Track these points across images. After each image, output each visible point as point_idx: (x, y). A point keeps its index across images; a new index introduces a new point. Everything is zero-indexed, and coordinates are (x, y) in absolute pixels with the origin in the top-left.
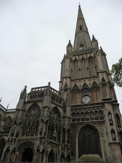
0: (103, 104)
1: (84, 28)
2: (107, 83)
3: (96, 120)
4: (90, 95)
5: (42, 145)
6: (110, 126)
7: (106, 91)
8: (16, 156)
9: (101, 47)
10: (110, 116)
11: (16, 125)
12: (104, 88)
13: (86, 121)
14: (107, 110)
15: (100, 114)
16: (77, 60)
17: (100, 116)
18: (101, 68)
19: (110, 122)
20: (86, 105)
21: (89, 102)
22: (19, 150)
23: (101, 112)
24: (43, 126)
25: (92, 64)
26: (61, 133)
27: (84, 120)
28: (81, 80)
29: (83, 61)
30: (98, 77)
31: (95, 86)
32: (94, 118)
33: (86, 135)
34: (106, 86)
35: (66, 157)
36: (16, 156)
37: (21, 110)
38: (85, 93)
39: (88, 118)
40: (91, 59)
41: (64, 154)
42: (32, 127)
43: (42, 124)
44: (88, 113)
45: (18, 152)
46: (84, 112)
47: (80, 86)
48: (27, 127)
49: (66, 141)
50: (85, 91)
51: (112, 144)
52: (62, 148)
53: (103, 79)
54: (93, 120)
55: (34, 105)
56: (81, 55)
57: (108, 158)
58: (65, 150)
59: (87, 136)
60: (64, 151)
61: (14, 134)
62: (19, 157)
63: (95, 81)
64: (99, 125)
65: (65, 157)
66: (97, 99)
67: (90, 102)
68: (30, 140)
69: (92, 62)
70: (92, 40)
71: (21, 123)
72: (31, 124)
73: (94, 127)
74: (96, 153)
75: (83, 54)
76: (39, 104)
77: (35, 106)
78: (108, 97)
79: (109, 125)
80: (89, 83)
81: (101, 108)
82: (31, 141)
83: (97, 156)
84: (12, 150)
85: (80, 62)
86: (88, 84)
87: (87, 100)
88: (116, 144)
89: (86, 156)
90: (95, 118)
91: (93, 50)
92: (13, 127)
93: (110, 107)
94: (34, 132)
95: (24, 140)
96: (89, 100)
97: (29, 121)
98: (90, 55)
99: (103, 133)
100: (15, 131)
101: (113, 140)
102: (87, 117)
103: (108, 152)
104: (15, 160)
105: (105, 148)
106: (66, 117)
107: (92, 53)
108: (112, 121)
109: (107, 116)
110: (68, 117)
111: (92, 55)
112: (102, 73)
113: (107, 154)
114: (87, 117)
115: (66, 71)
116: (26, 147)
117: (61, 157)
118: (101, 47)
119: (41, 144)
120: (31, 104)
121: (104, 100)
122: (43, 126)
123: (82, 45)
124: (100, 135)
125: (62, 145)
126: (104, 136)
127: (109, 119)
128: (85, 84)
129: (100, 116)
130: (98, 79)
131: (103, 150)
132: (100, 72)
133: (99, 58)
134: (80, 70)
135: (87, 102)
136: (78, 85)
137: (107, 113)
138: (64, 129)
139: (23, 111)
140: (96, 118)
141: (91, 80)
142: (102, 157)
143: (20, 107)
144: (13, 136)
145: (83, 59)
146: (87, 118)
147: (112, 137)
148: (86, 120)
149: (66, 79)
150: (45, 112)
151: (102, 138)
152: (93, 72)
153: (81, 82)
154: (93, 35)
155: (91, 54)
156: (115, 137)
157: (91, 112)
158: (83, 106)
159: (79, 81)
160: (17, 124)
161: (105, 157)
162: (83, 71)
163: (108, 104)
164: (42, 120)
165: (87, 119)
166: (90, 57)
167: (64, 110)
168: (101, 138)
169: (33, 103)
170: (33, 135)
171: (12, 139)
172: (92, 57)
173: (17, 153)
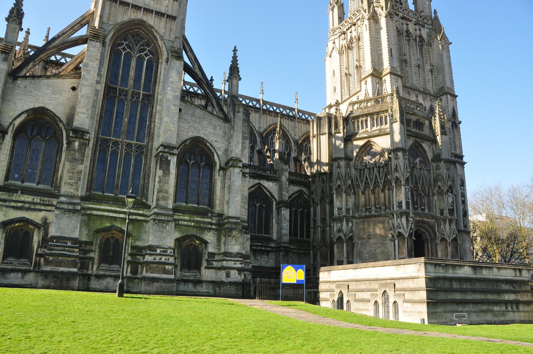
76: (425, 145)
82: (428, 220)
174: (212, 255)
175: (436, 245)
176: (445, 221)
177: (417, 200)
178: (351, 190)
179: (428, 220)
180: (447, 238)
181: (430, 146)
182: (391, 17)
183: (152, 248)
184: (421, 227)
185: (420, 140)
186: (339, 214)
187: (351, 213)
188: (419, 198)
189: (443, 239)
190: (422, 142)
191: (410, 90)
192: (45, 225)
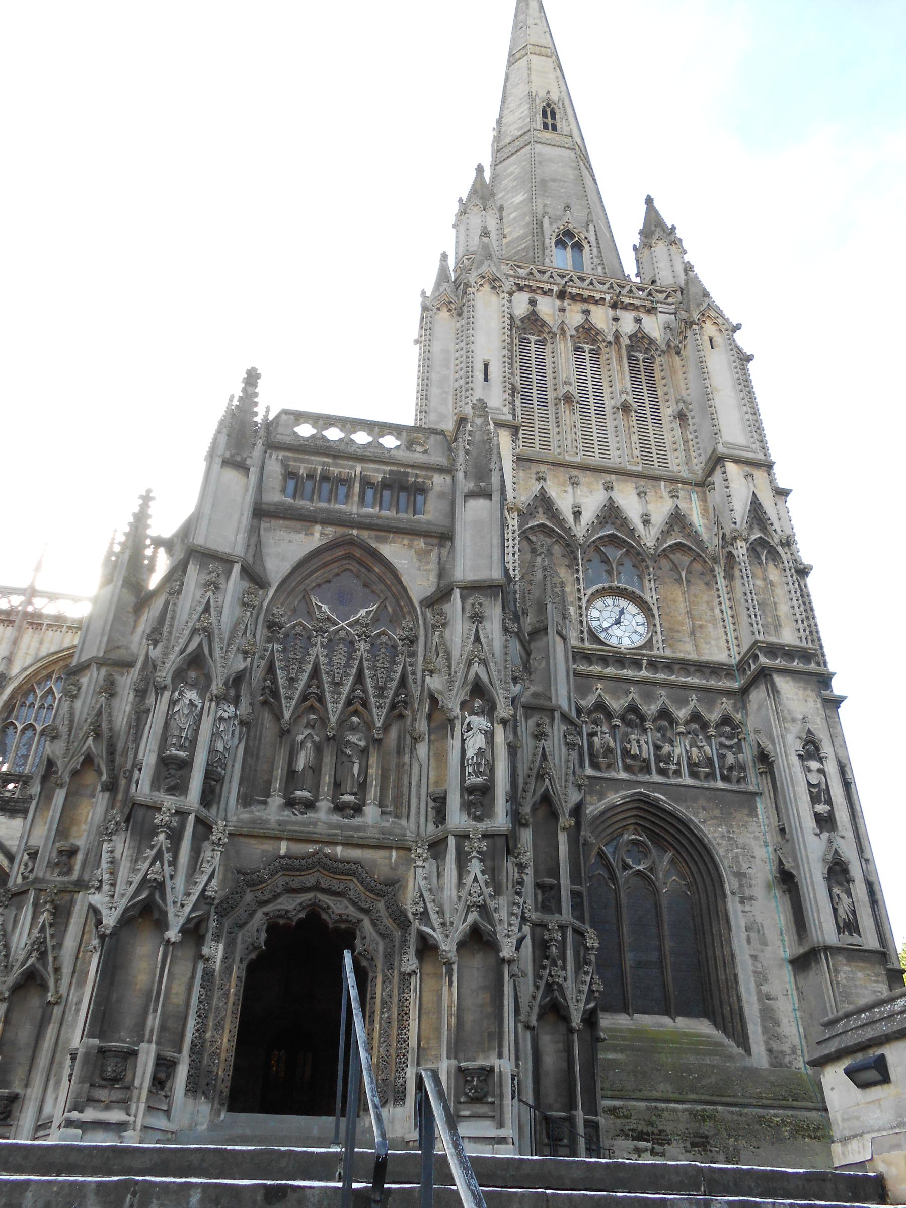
0: (764, 675)
2: (782, 544)
3: (694, 775)
4: (650, 597)
5: (503, 901)
6: (816, 834)
7: (772, 591)
8: (208, 975)
10: (814, 765)
11: (203, 687)
12: (758, 571)
13: (623, 775)
14: (794, 720)
15: (723, 740)
16: (544, 324)
17: (722, 757)
19: (822, 808)
20: (620, 659)
21: (639, 641)
22: (227, 922)
23: (728, 729)
24: (490, 736)
25: (652, 388)
26: (526, 825)
27: (609, 766)
28: (585, 478)
29: (587, 347)
30: (703, 484)
31: (679, 546)
32: (678, 764)
33: (622, 876)
34: (771, 565)
35: (576, 1020)
36: (208, 975)
37: (237, 568)
38: (609, 573)
39: (645, 755)
40: (641, 356)
41: (566, 1000)
42: (337, 741)
43: (479, 722)
44: (642, 718)
45: (221, 947)
46: (616, 704)
47: (577, 514)
48: (284, 733)
49: (565, 894)
50: (606, 561)
51: (841, 959)
52: (542, 947)
54: (677, 773)
55: (340, 552)
56: (575, 298)
57: (786, 1048)
58: (564, 968)
59: (627, 882)
60: (563, 973)
61: (186, 765)
62: (226, 995)
63: (682, 505)
64: (717, 813)
65: (565, 1019)
66: (693, 633)
67: (649, 644)
68: (347, 844)
69: (650, 372)
71: (238, 680)
72: (334, 710)
73: (685, 824)
74: (688, 1014)
76: (396, 552)
77: (350, 560)
78: (788, 637)
79: (809, 823)
80: (646, 511)
81: (726, 705)
82: (356, 853)
83: (703, 1027)
84: (189, 920)
87: (623, 628)
88: (863, 960)
90: (691, 765)
91: (661, 297)
92: (173, 703)
93: (811, 704)
94: (363, 786)
95: (281, 839)
96: (641, 629)
97: (304, 677)
98: (638, 320)
99: (744, 875)
100: (193, 742)
101: (839, 933)
102: (643, 745)
103: (786, 1009)
104: (202, 1016)
105: (761, 978)
106: (550, 711)
107: (650, 311)
108: (829, 802)
109: (795, 760)
110: (565, 718)
111: (654, 326)
112: (748, 469)
113: (777, 1023)
114: (643, 745)
115: (480, 376)
116: (290, 905)
117: (540, 1017)
119: (498, 892)
120: (316, 537)
121: (773, 650)
122: (490, 736)
123: (569, 233)
124: (730, 884)
126: (751, 898)
127: (810, 784)
128: (611, 513)
129: (722, 757)
130: (704, 500)
131: (748, 989)
132: (737, 461)
133: (718, 364)
134: (568, 398)
135: (626, 642)
137: (794, 745)
138: (546, 799)
139: (254, 577)
140: (697, 765)
141: (651, 495)
142: (743, 1041)
143: (230, 538)
144: (179, 788)
145: (588, 332)
146: (635, 750)
147: (835, 910)
148: (628, 768)
150: (487, 624)
151: (739, 907)
152: (661, 447)
153: (581, 491)
156: (854, 912)
157: (664, 714)
158: (604, 660)
159: (563, 474)
160: (217, 687)
161: (767, 1043)
162: (585, 415)
163: (793, 678)
164: (478, 689)
165: (634, 757)
167: (524, 655)
168: (733, 906)
169: (330, 530)
170: (358, 809)
171: (181, 814)
172: (652, 341)
173: (215, 951)
175: (406, 977)
176: (437, 847)
177: (315, 769)
178: (100, 773)
179: (356, 853)
180: (437, 935)
181: (422, 555)
182: (494, 288)
184: (317, 888)
185: (365, 535)
186: (24, 878)
187: (77, 867)
188: (328, 760)
189: (427, 948)
190: (384, 540)
191: (575, 472)
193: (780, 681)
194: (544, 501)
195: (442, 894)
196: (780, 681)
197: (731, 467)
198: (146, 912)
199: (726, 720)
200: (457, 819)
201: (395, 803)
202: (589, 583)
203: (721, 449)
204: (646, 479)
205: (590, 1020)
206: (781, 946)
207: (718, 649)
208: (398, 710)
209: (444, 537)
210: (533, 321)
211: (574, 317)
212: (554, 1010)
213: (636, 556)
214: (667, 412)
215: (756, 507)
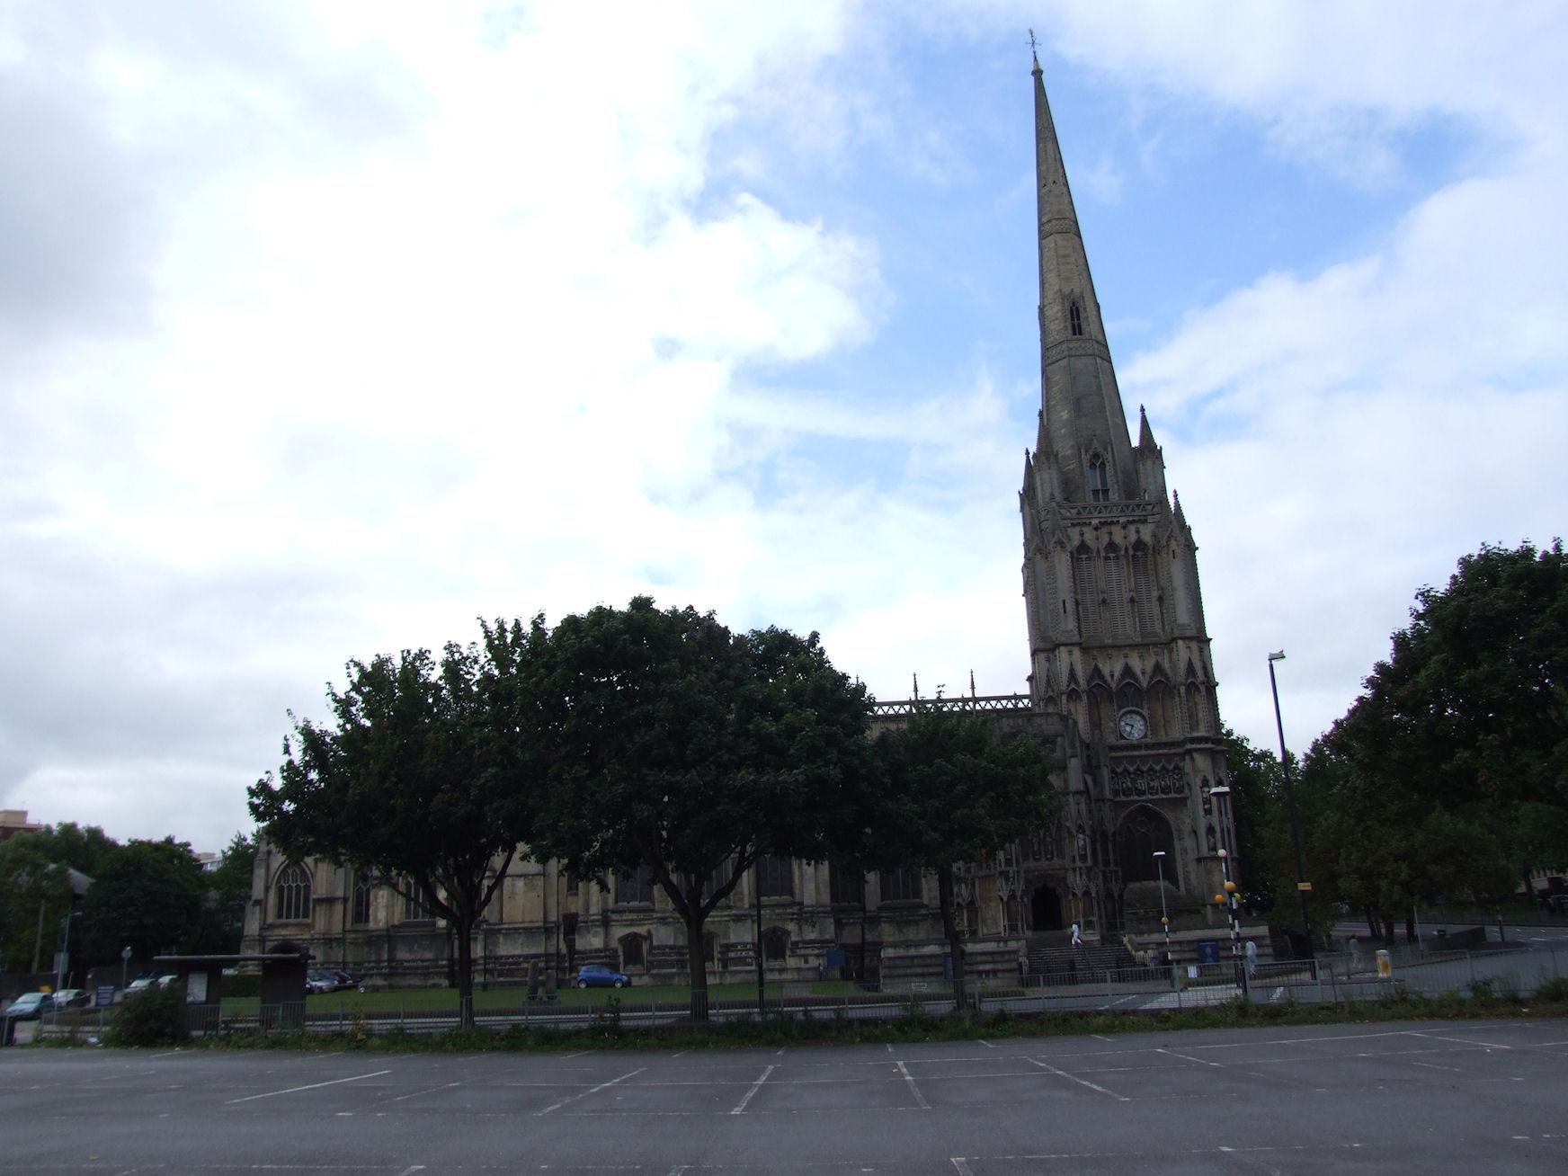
1: (1089, 328)
4: (1145, 713)
9: (1176, 496)
18: (1183, 617)
53: (1190, 669)
70: (1135, 442)
75: (1112, 523)
78: (1201, 733)
79: (1202, 813)
85: (1100, 563)
86: (1139, 673)
87: (1135, 729)
89: (1137, 885)
102: (1141, 784)
105: (1185, 866)
107: (1144, 522)
111: (1146, 533)
114: (1141, 784)
118: (1176, 496)
121: (1193, 740)
123: (1096, 456)
124: (1175, 834)
125: (1104, 872)
128: (1127, 671)
132: (1183, 639)
136: (1106, 671)
137: (1199, 783)
145: (1112, 546)
149: (1070, 653)
154: (1143, 410)
155: (1142, 527)
157: (1151, 769)
166: (1139, 545)
174: (795, 944)
183: (735, 945)
192: (649, 936)
193: (1195, 755)
194: (1097, 671)
195: (1077, 882)
196: (1195, 755)
197: (1180, 643)
198: (1012, 896)
199: (1176, 767)
200: (1079, 864)
201: (1061, 855)
202: (1120, 708)
203: (1177, 633)
204: (1142, 647)
205: (1121, 896)
206: (1192, 855)
207: (1177, 733)
208: (1059, 829)
209: (1064, 768)
210: (1083, 548)
211: (1106, 539)
212: (1109, 895)
213: (1139, 691)
214: (1155, 594)
215: (1190, 664)
